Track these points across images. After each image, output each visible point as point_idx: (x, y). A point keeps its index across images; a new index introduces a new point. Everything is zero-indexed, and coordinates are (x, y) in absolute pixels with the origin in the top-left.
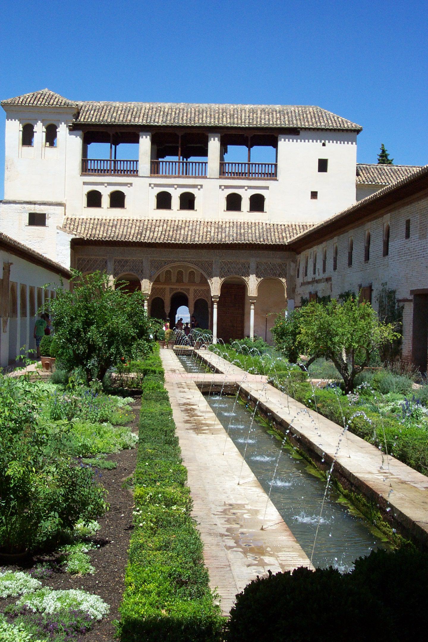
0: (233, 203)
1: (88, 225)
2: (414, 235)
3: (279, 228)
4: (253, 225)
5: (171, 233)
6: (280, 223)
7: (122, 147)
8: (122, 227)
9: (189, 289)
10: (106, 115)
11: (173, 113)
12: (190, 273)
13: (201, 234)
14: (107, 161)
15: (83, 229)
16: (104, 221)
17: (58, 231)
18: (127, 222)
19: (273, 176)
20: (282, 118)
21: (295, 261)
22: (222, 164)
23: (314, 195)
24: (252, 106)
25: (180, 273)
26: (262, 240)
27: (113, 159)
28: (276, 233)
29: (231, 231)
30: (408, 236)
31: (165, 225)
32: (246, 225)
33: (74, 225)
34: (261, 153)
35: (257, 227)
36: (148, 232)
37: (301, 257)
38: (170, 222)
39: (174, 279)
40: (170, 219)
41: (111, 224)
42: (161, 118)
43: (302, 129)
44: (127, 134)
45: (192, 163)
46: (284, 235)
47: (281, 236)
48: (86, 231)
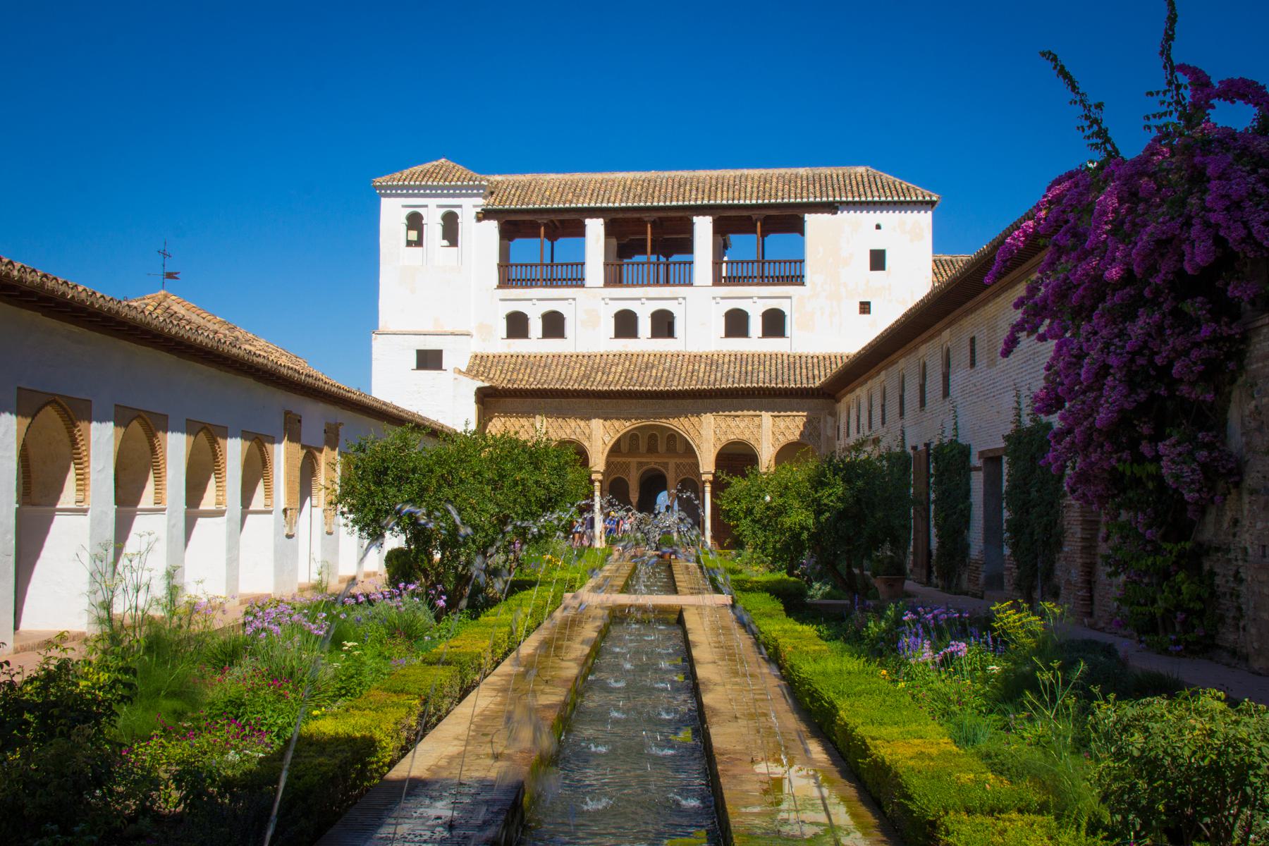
0: (736, 324)
2: (982, 361)
5: (635, 375)
6: (811, 353)
7: (563, 244)
9: (667, 464)
17: (457, 376)
18: (567, 360)
20: (811, 187)
21: (833, 414)
22: (717, 264)
23: (865, 308)
24: (763, 171)
25: (653, 438)
26: (779, 380)
27: (547, 260)
28: (804, 371)
29: (732, 369)
30: (973, 364)
32: (756, 359)
34: (777, 244)
37: (841, 407)
39: (643, 447)
43: (841, 203)
44: (568, 224)
46: (816, 372)
47: (810, 375)
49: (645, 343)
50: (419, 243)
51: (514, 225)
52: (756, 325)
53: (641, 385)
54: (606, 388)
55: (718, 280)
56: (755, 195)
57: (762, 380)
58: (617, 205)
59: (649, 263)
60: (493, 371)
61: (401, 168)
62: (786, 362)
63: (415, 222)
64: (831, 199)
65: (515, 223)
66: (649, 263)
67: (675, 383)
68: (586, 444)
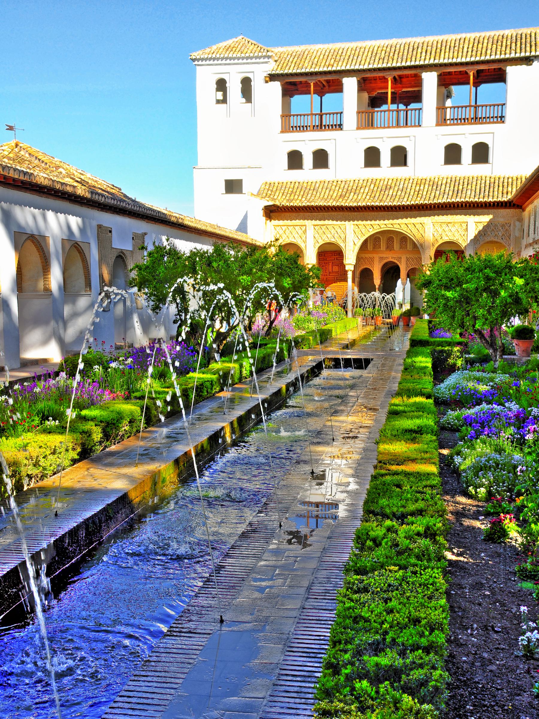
0: (453, 154)
1: (287, 189)
3: (506, 181)
4: (475, 180)
7: (328, 97)
8: (324, 190)
9: (401, 258)
10: (307, 61)
11: (383, 52)
12: (401, 239)
13: (412, 193)
14: (308, 115)
15: (281, 194)
16: (305, 185)
19: (501, 119)
20: (514, 45)
22: (441, 108)
24: (477, 35)
28: (501, 188)
29: (447, 189)
31: (372, 186)
32: (466, 181)
33: (272, 191)
35: (479, 182)
36: (352, 194)
37: (526, 213)
38: (378, 182)
40: (379, 178)
41: (312, 188)
42: (368, 60)
44: (329, 83)
45: (412, 110)
47: (505, 191)
48: (284, 197)
49: (386, 171)
50: (224, 101)
51: (293, 85)
52: (467, 155)
53: (381, 201)
54: (355, 204)
55: (442, 121)
56: (469, 53)
57: (469, 197)
58: (366, 67)
59: (389, 110)
60: (277, 194)
61: (209, 46)
62: (488, 182)
63: (221, 85)
64: (528, 54)
65: (294, 84)
66: (389, 110)
67: (405, 199)
68: (342, 245)
